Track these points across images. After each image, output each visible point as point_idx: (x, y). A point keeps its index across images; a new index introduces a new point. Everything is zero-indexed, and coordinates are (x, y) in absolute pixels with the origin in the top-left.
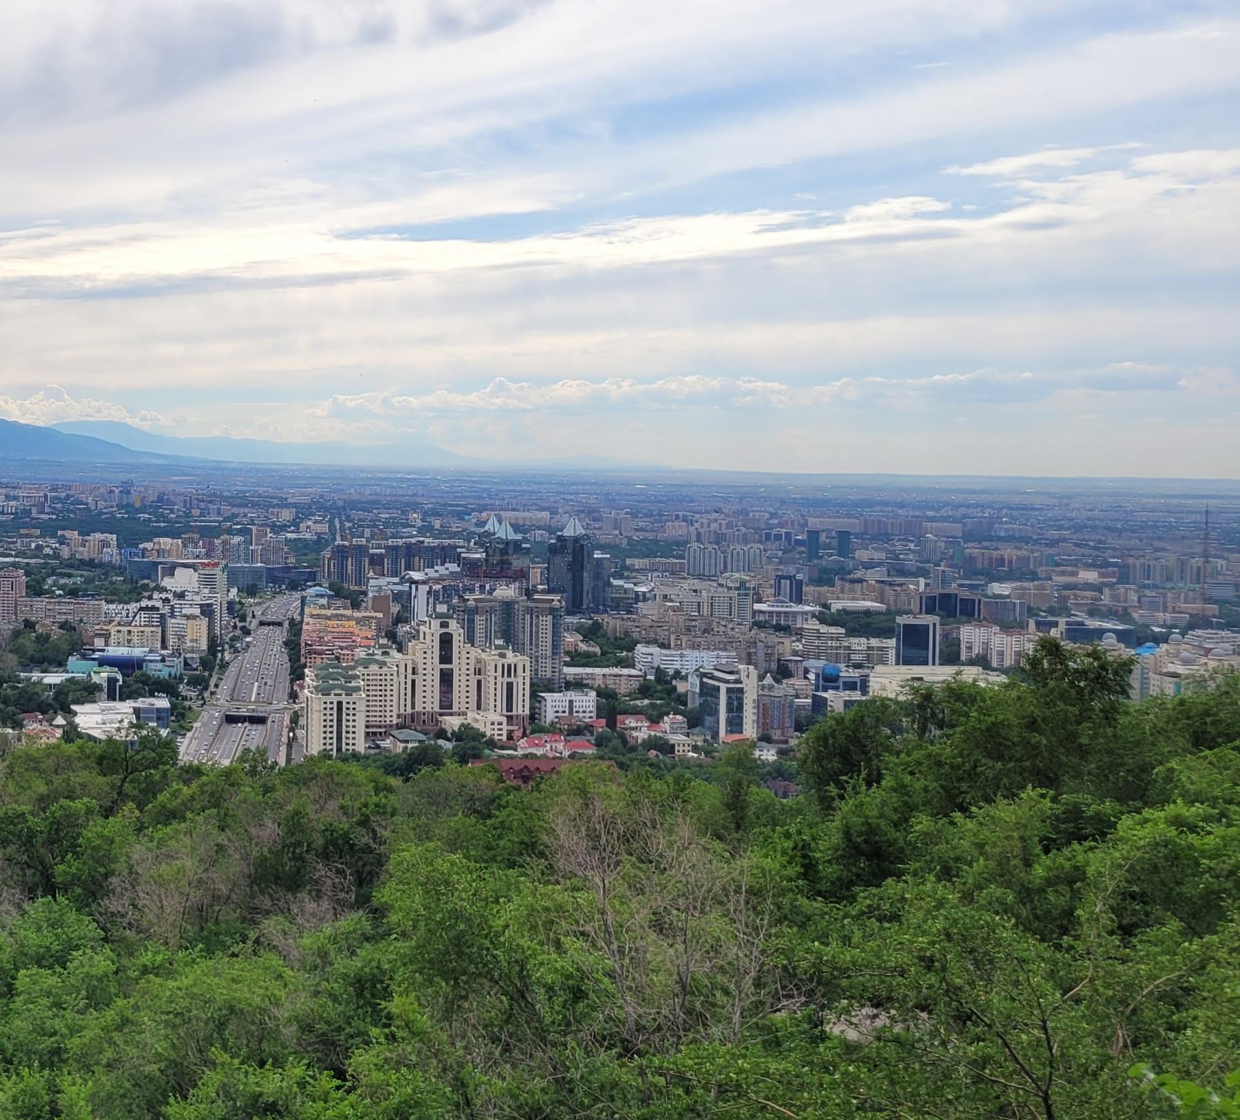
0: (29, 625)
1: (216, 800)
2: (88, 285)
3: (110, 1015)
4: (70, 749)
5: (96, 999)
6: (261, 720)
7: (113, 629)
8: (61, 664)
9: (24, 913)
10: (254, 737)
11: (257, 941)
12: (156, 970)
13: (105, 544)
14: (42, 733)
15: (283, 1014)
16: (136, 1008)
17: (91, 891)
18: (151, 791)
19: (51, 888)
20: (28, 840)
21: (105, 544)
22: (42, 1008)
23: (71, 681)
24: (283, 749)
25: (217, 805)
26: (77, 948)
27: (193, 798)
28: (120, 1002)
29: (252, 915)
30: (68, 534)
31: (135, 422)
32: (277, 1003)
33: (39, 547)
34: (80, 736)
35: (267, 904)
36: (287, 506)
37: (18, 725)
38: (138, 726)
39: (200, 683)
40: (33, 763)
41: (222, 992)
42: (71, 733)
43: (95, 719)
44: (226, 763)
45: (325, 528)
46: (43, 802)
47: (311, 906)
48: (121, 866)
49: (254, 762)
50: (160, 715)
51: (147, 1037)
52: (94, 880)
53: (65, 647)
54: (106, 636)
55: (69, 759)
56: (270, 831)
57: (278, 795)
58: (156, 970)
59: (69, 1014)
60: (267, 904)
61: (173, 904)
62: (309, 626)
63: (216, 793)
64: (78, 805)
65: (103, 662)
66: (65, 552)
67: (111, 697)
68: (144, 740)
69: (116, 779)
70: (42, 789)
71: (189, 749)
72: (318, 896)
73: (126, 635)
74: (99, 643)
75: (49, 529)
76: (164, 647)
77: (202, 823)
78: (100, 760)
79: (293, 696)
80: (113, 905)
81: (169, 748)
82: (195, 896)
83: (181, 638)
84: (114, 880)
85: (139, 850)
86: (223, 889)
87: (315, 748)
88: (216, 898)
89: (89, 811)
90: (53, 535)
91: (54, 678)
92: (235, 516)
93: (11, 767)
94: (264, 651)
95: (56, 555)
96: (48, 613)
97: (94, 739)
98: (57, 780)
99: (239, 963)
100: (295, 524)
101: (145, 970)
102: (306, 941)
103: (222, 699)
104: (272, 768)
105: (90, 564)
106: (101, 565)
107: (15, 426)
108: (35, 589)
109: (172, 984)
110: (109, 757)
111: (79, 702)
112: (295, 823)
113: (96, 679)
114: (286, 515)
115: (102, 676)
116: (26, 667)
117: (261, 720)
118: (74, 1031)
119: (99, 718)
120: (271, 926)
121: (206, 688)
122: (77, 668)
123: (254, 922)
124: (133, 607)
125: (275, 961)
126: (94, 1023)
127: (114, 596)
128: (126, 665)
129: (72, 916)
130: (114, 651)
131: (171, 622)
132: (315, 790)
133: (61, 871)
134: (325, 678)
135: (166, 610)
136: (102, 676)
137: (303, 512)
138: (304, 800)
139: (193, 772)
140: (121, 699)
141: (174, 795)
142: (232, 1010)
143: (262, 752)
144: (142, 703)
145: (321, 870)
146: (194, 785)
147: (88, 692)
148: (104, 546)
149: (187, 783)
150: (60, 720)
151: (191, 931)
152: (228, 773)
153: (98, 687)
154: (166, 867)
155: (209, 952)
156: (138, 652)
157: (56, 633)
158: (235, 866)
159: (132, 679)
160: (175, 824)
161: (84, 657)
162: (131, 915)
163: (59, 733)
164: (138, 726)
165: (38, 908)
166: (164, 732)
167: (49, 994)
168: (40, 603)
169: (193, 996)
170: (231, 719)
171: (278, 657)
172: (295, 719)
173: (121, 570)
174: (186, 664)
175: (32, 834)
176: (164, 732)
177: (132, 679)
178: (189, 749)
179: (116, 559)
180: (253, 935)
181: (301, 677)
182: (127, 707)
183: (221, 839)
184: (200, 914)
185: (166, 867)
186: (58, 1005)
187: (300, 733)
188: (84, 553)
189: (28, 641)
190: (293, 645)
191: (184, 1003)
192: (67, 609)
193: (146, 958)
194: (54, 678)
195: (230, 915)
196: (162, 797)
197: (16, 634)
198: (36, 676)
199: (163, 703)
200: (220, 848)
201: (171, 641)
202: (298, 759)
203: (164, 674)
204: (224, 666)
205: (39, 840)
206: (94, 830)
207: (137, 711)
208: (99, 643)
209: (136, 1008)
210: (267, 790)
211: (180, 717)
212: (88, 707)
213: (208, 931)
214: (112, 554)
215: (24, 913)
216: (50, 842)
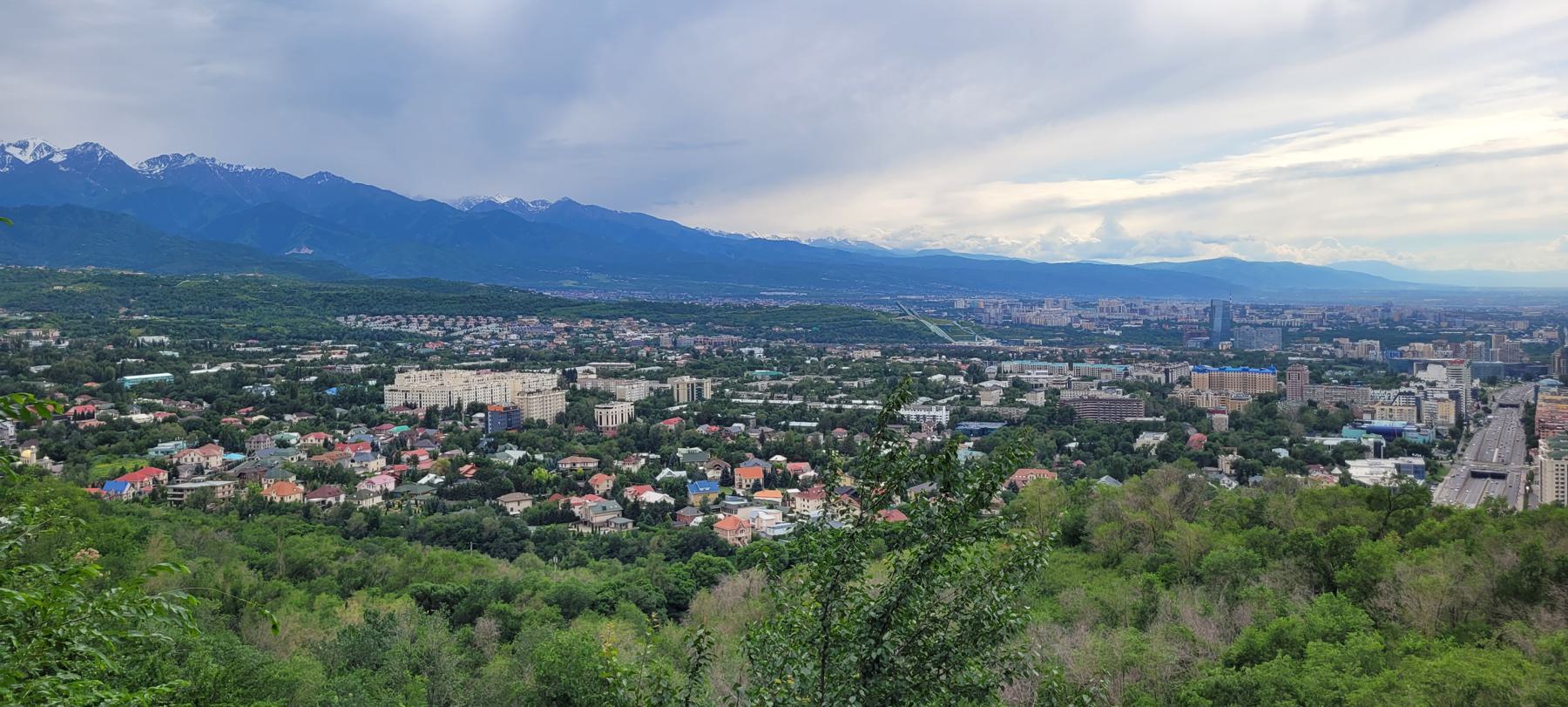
0: (1312, 404)
1: (1463, 533)
2: (1355, 166)
3: (1380, 680)
4: (1346, 491)
5: (1369, 667)
6: (1502, 477)
7: (1378, 408)
8: (1337, 431)
9: (1311, 603)
10: (1496, 489)
11: (1500, 638)
12: (1417, 652)
13: (1370, 347)
14: (1324, 479)
15: (1524, 692)
16: (1400, 677)
17: (1364, 592)
18: (1409, 524)
19: (1333, 588)
20: (1314, 552)
21: (1370, 347)
22: (1326, 670)
23: (1345, 443)
24: (1521, 500)
25: (1464, 536)
26: (1353, 630)
27: (1444, 530)
28: (1388, 672)
29: (1495, 619)
30: (1341, 340)
31: (1394, 261)
32: (1517, 685)
33: (1319, 350)
34: (1353, 482)
35: (1508, 611)
36: (1522, 319)
37: (1304, 472)
38: (1400, 477)
39: (1450, 448)
40: (1317, 499)
41: (1471, 673)
42: (1346, 480)
43: (1363, 471)
44: (1473, 506)
45: (1556, 334)
46: (1325, 527)
47: (1546, 616)
48: (1387, 575)
49: (1495, 508)
50: (1417, 471)
51: (1409, 698)
52: (1366, 584)
53: (1340, 420)
54: (1373, 413)
55: (1344, 498)
56: (1510, 558)
57: (1518, 531)
58: (1417, 652)
59: (1347, 676)
60: (1508, 611)
61: (1429, 606)
62: (1542, 409)
63: (1464, 528)
64: (1352, 530)
65: (1369, 431)
66: (1339, 353)
67: (1377, 455)
68: (1404, 489)
69: (1382, 514)
70: (1324, 517)
71: (1441, 495)
72: (1553, 609)
73: (1388, 411)
74: (1367, 417)
75: (1326, 337)
76: (1419, 420)
77: (1454, 549)
78: (1369, 500)
79: (1529, 460)
80: (1381, 602)
81: (1425, 494)
82: (1447, 602)
83: (1433, 415)
84: (1381, 585)
85: (1401, 565)
86: (1471, 598)
87: (1549, 497)
88: (1465, 604)
89: (1361, 535)
90: (1330, 341)
91: (1332, 441)
92: (1477, 326)
93: (1300, 501)
94: (1504, 428)
95: (1332, 356)
96: (1327, 396)
97: (1361, 484)
98: (1336, 513)
99: (1485, 653)
100: (1530, 333)
101: (1408, 651)
102: (1543, 641)
103: (1469, 459)
104: (1511, 512)
105: (1359, 362)
106: (1368, 362)
107: (1300, 267)
108: (1316, 379)
109: (1429, 663)
110: (1375, 498)
111: (1351, 458)
112: (1532, 554)
113: (1364, 442)
114: (1521, 326)
115: (1370, 441)
116: (1310, 433)
117: (1502, 477)
118: (1351, 688)
119: (1368, 470)
120: (1514, 628)
121: (1454, 451)
122: (1349, 435)
123: (1497, 624)
124: (1394, 392)
125: (1516, 655)
126: (1367, 686)
127: (1377, 384)
128: (1388, 434)
129: (1349, 608)
130: (1378, 423)
131: (1424, 403)
132: (1548, 530)
133: (1340, 576)
134: (1557, 447)
135: (1421, 394)
136: (1370, 441)
137: (1535, 323)
138: (1540, 538)
139: (1443, 512)
140: (1386, 457)
141: (1429, 527)
142: (1479, 686)
143: (1503, 500)
144: (1401, 460)
145: (1555, 590)
146: (1445, 521)
147: (1359, 452)
148: (1372, 349)
149: (1440, 519)
150: (1337, 470)
151: (1445, 626)
152: (1473, 515)
153: (1367, 449)
154: (1425, 579)
155: (1460, 642)
156: (1398, 424)
157: (1333, 410)
158: (1480, 583)
159: (1393, 443)
160: (1430, 549)
161: (1355, 427)
162: (1395, 611)
163: (1336, 480)
164: (1400, 477)
165: (1323, 600)
166: (1420, 482)
167: (1331, 660)
168: (1321, 389)
169: (1447, 674)
170: (1475, 475)
171: (1516, 432)
172: (1531, 477)
173: (1383, 366)
174: (1438, 434)
175: (1316, 549)
176: (1420, 482)
177: (1393, 443)
178: (1441, 495)
179: (1380, 358)
180: (1496, 633)
181: (1536, 445)
182: (1390, 463)
183: (1469, 561)
184: (1452, 615)
185: (1425, 579)
186: (1339, 669)
187: (1536, 487)
188: (1353, 354)
189: (1312, 415)
190: (1529, 422)
191: (1439, 678)
192: (1341, 393)
193: (1408, 642)
194: (1332, 441)
195: (1477, 618)
196: (1420, 528)
197: (1303, 410)
198: (1318, 439)
199: (1419, 461)
200: (1468, 568)
201: (1425, 417)
202: (1534, 506)
203: (1420, 440)
204: (1469, 436)
205: (1322, 553)
206: (1365, 548)
207: (1398, 467)
208: (1367, 417)
209: (1400, 677)
210: (1507, 528)
211: (1433, 471)
212: (1359, 462)
213: (1458, 626)
214: (1376, 354)
215: (1311, 603)
216: (1331, 555)
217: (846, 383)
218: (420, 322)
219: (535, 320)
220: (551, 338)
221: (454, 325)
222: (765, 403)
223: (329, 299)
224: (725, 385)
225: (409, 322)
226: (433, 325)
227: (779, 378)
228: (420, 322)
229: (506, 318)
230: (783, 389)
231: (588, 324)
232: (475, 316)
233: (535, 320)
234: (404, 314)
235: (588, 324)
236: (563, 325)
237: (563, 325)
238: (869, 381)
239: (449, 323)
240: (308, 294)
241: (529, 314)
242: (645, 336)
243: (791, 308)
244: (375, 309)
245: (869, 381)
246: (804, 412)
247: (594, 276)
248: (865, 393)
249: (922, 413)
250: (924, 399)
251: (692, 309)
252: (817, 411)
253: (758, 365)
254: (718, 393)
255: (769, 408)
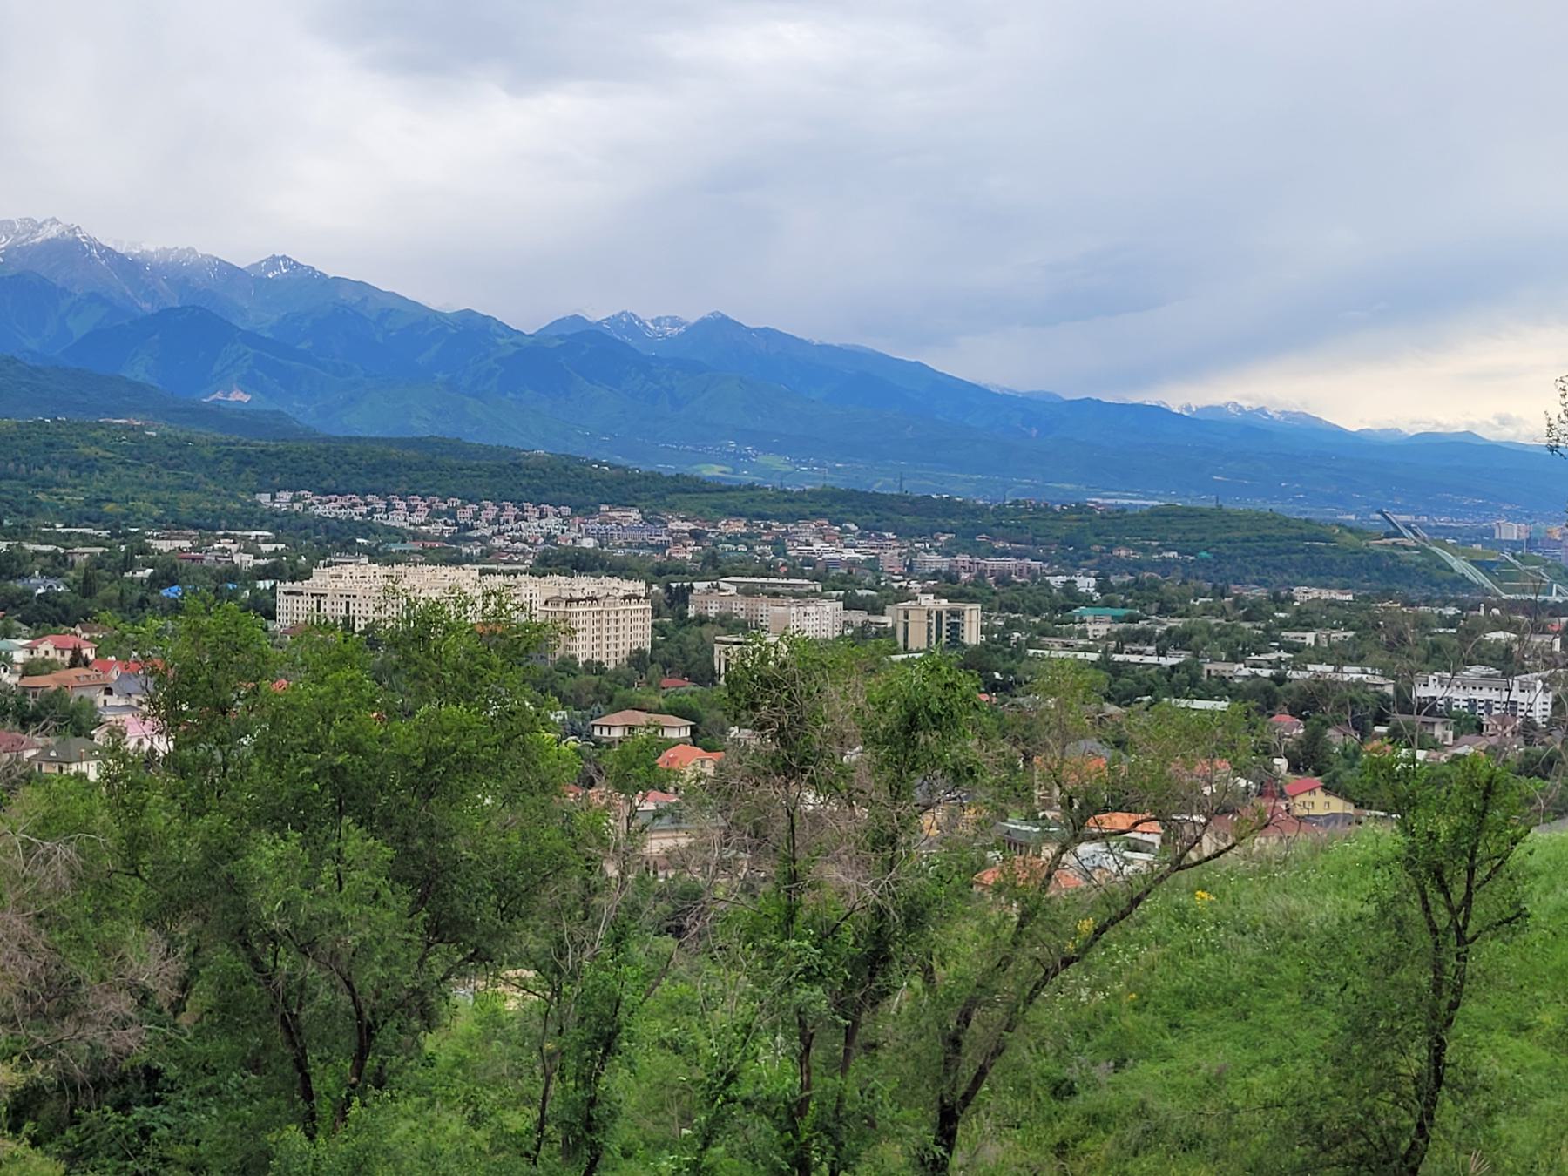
217: (1289, 635)
218: (412, 510)
219: (635, 514)
220: (661, 547)
221: (476, 517)
222: (1105, 664)
223: (245, 461)
224: (1011, 626)
225: (390, 507)
226: (435, 515)
227: (1133, 619)
228: (412, 510)
229: (576, 509)
230: (1145, 637)
231: (739, 527)
232: (518, 503)
233: (635, 514)
234: (383, 494)
235: (739, 527)
236: (688, 526)
237: (688, 526)
238: (1338, 635)
239: (465, 515)
240: (208, 453)
241: (624, 503)
242: (849, 554)
243: (1155, 512)
244: (329, 483)
245: (1338, 635)
246: (1194, 681)
247: (764, 459)
248: (1340, 656)
249: (1481, 695)
250: (1477, 669)
251: (948, 508)
252: (1224, 681)
253: (1087, 601)
254: (997, 642)
255: (1117, 670)
